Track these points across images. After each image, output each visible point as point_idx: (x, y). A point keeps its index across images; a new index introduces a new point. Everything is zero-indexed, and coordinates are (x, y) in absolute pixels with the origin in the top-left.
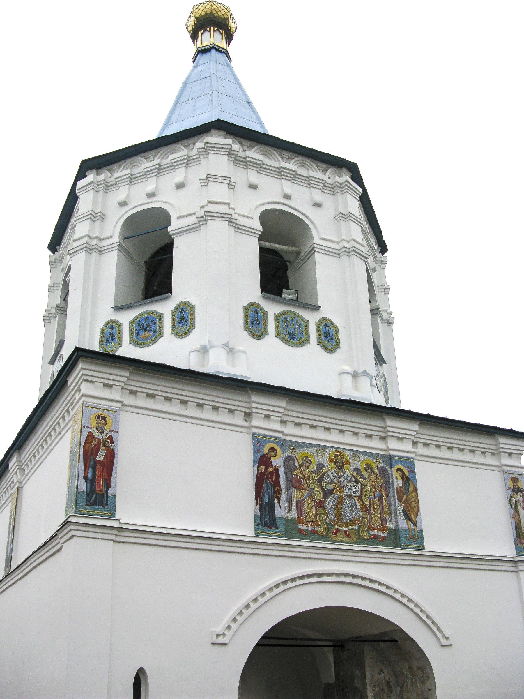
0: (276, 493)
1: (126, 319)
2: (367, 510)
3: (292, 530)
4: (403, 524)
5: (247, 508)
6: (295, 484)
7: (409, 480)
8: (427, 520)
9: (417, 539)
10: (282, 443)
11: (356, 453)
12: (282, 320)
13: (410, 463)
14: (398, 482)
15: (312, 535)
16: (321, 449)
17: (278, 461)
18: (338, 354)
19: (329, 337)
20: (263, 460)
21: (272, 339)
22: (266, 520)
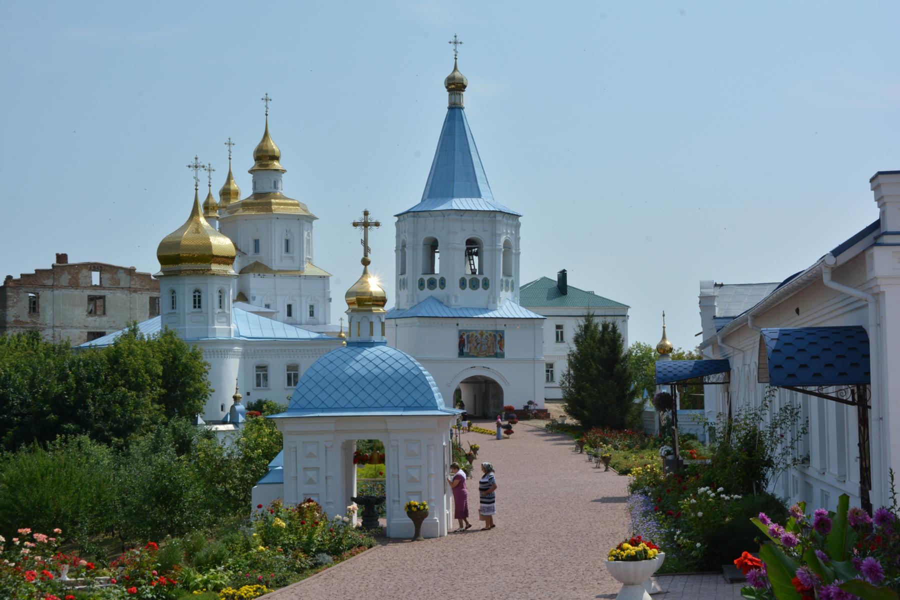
0: (464, 346)
1: (426, 278)
2: (489, 347)
3: (468, 355)
4: (499, 351)
5: (456, 350)
6: (469, 342)
7: (502, 338)
8: (506, 349)
9: (502, 356)
10: (467, 331)
11: (487, 331)
12: (471, 281)
13: (503, 332)
14: (498, 338)
15: (473, 356)
16: (477, 331)
17: (465, 337)
18: (489, 289)
19: (486, 284)
20: (461, 337)
21: (468, 289)
22: (461, 354)
